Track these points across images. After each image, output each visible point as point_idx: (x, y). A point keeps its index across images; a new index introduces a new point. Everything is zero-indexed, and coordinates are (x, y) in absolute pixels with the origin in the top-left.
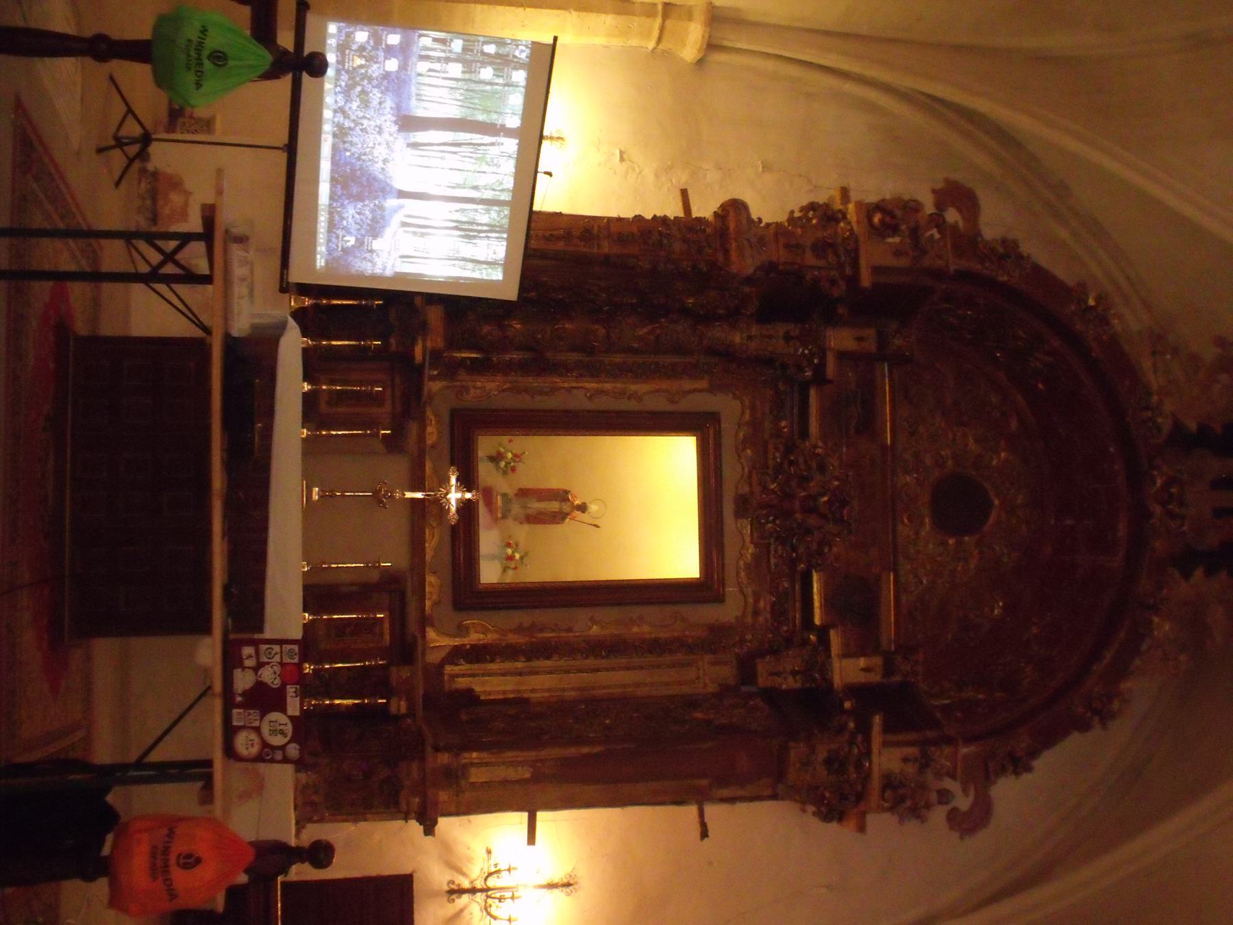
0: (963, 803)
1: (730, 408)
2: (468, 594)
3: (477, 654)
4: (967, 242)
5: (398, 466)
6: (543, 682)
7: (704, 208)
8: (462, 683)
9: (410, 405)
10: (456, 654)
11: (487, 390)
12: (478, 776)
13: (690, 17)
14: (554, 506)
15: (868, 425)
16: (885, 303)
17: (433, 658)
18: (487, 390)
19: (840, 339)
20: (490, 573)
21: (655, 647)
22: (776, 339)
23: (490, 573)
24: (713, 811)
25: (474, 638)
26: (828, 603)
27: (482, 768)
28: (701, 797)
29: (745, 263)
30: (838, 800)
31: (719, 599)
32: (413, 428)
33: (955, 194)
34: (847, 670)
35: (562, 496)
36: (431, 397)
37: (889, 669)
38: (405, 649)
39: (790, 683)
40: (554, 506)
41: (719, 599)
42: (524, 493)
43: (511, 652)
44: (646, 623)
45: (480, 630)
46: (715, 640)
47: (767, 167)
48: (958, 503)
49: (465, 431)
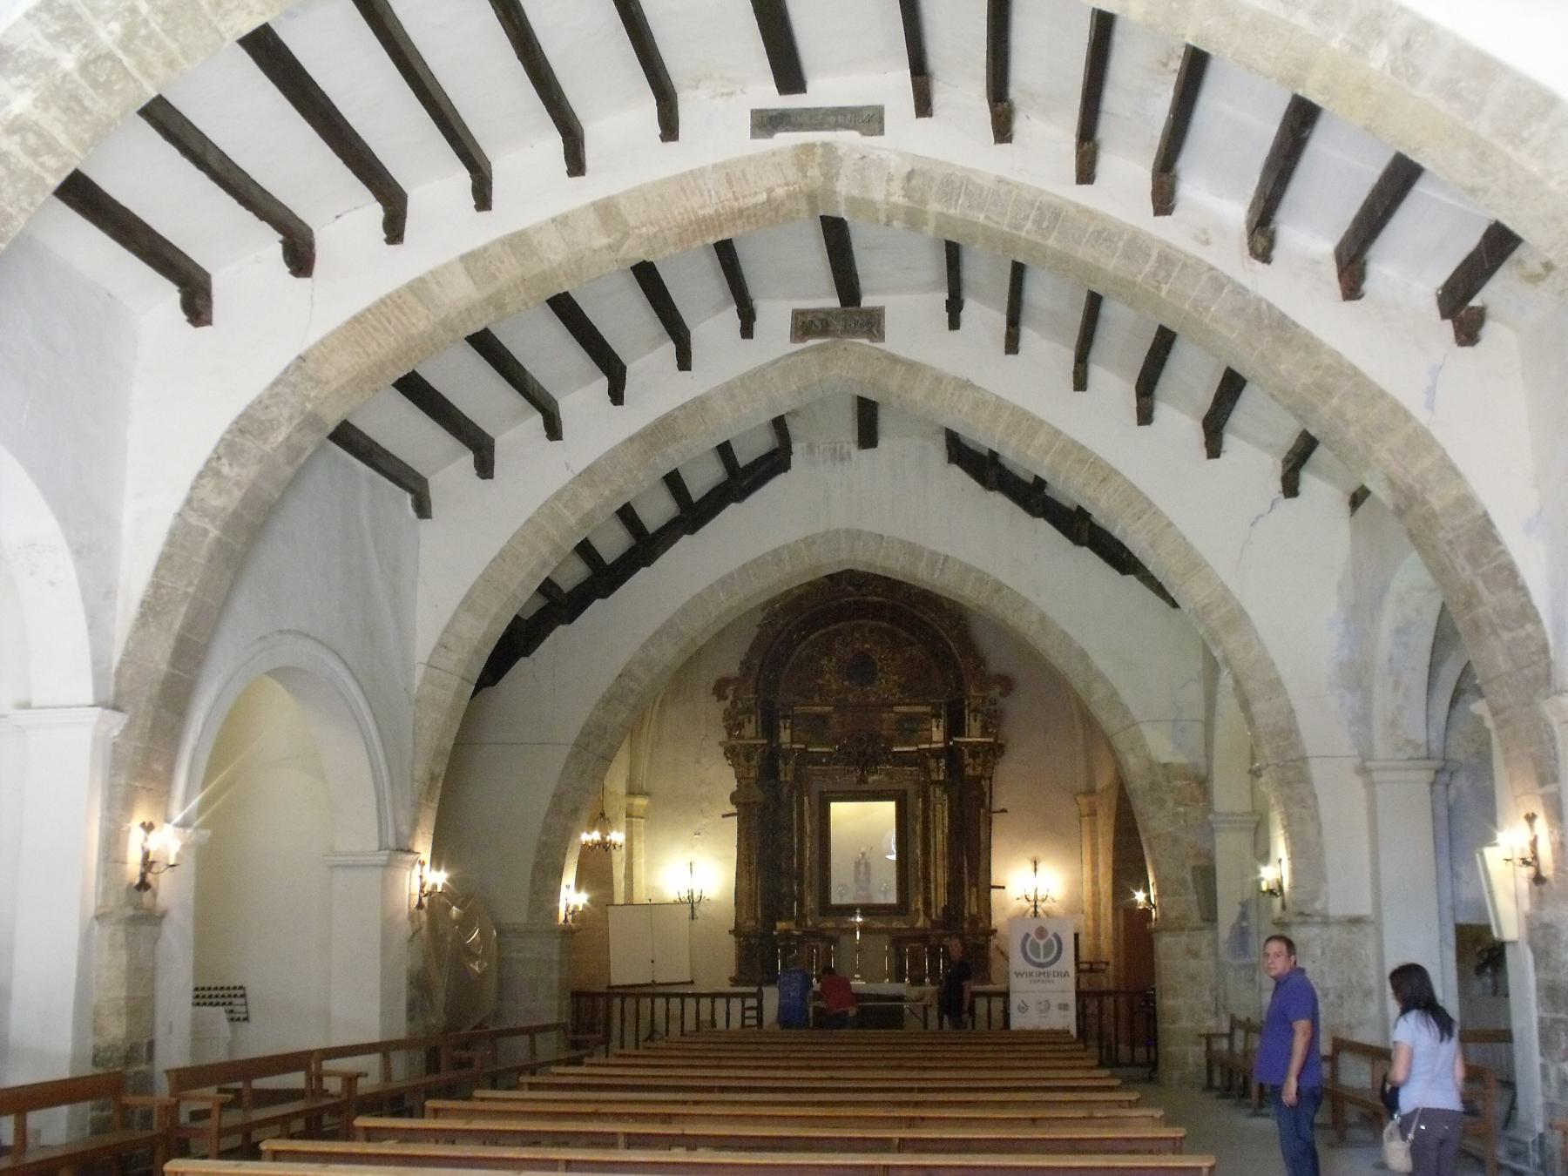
0: (998, 689)
2: (901, 908)
3: (927, 904)
5: (844, 939)
6: (940, 875)
8: (940, 911)
9: (819, 934)
10: (927, 914)
11: (810, 902)
12: (974, 910)
13: (631, 805)
14: (862, 868)
15: (824, 718)
17: (929, 925)
18: (810, 902)
19: (785, 736)
20: (892, 899)
23: (892, 899)
24: (997, 806)
25: (920, 906)
26: (907, 743)
27: (972, 908)
28: (990, 811)
29: (758, 796)
31: (905, 793)
32: (828, 934)
33: (720, 689)
34: (938, 735)
35: (857, 864)
36: (815, 925)
37: (938, 716)
38: (923, 937)
40: (862, 868)
42: (856, 880)
43: (927, 890)
47: (698, 762)
48: (862, 669)
49: (826, 908)
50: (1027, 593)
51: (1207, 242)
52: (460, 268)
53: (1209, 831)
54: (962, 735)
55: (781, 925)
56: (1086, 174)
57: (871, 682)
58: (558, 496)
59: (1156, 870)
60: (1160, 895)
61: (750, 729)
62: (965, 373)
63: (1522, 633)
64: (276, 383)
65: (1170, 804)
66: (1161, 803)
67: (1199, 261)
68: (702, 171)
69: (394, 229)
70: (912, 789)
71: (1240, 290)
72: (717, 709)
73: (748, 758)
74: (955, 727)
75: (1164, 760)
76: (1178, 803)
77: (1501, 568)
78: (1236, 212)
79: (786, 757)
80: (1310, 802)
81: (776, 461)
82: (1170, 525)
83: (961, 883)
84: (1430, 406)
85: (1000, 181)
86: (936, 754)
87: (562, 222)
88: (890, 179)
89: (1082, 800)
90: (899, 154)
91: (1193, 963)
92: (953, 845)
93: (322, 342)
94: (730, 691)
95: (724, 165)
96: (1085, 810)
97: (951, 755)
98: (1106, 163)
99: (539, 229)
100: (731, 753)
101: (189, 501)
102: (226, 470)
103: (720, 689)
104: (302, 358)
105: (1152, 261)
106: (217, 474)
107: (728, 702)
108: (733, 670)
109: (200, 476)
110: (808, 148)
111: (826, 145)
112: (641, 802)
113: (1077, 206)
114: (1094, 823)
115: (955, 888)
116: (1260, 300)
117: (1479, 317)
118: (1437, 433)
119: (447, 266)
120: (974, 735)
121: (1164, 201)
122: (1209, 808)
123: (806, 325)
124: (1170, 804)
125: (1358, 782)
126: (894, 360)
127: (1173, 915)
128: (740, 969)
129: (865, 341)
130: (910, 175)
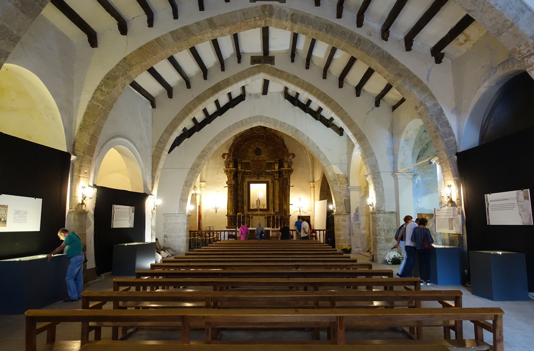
1: (247, 180)
2: (268, 210)
3: (274, 209)
4: (229, 155)
6: (277, 202)
7: (227, 185)
11: (246, 208)
15: (249, 163)
16: (236, 166)
19: (239, 167)
20: (265, 207)
21: (274, 189)
22: (240, 176)
23: (265, 207)
29: (233, 182)
30: (290, 171)
31: (268, 182)
37: (277, 163)
39: (278, 175)
41: (268, 182)
43: (274, 205)
44: (271, 190)
45: (271, 208)
46: (273, 182)
48: (258, 152)
49: (249, 210)
50: (304, 132)
51: (371, 35)
52: (170, 36)
53: (348, 190)
54: (283, 167)
55: (238, 214)
56: (339, 16)
57: (260, 154)
58: (190, 103)
59: (335, 200)
60: (336, 205)
61: (231, 166)
62: (295, 74)
63: (449, 139)
64: (118, 65)
65: (339, 184)
66: (337, 183)
67: (368, 40)
68: (236, 11)
69: (151, 23)
70: (270, 180)
71: (379, 48)
72: (223, 161)
73: (231, 173)
74: (281, 166)
75: (337, 173)
76: (341, 184)
77: (444, 122)
78: (378, 27)
79: (240, 173)
80: (381, 183)
81: (242, 98)
82: (346, 113)
83: (283, 204)
84: (428, 80)
85: (317, 17)
86: (276, 172)
87: (198, 24)
88: (287, 16)
89: (311, 184)
90: (290, 9)
91: (344, 223)
92: (280, 194)
93: (131, 54)
94: (226, 157)
95: (242, 10)
96: (312, 186)
97: (280, 172)
98: (345, 13)
99: (192, 25)
100: (226, 172)
101: (93, 98)
102: (104, 89)
103: (223, 156)
104: (125, 58)
105: (356, 40)
106: (101, 90)
107: (225, 159)
108: (227, 152)
109: (96, 90)
110: (265, 6)
111: (270, 5)
112: (203, 184)
113: (336, 24)
114: (314, 190)
115: (281, 205)
116: (384, 51)
117: (443, 55)
118: (428, 86)
119: (166, 35)
120: (286, 167)
121: (360, 23)
122: (348, 185)
123: (255, 60)
124: (339, 184)
125: (392, 178)
126: (277, 70)
127: (340, 211)
128: (228, 225)
129: (270, 65)
130: (292, 15)
